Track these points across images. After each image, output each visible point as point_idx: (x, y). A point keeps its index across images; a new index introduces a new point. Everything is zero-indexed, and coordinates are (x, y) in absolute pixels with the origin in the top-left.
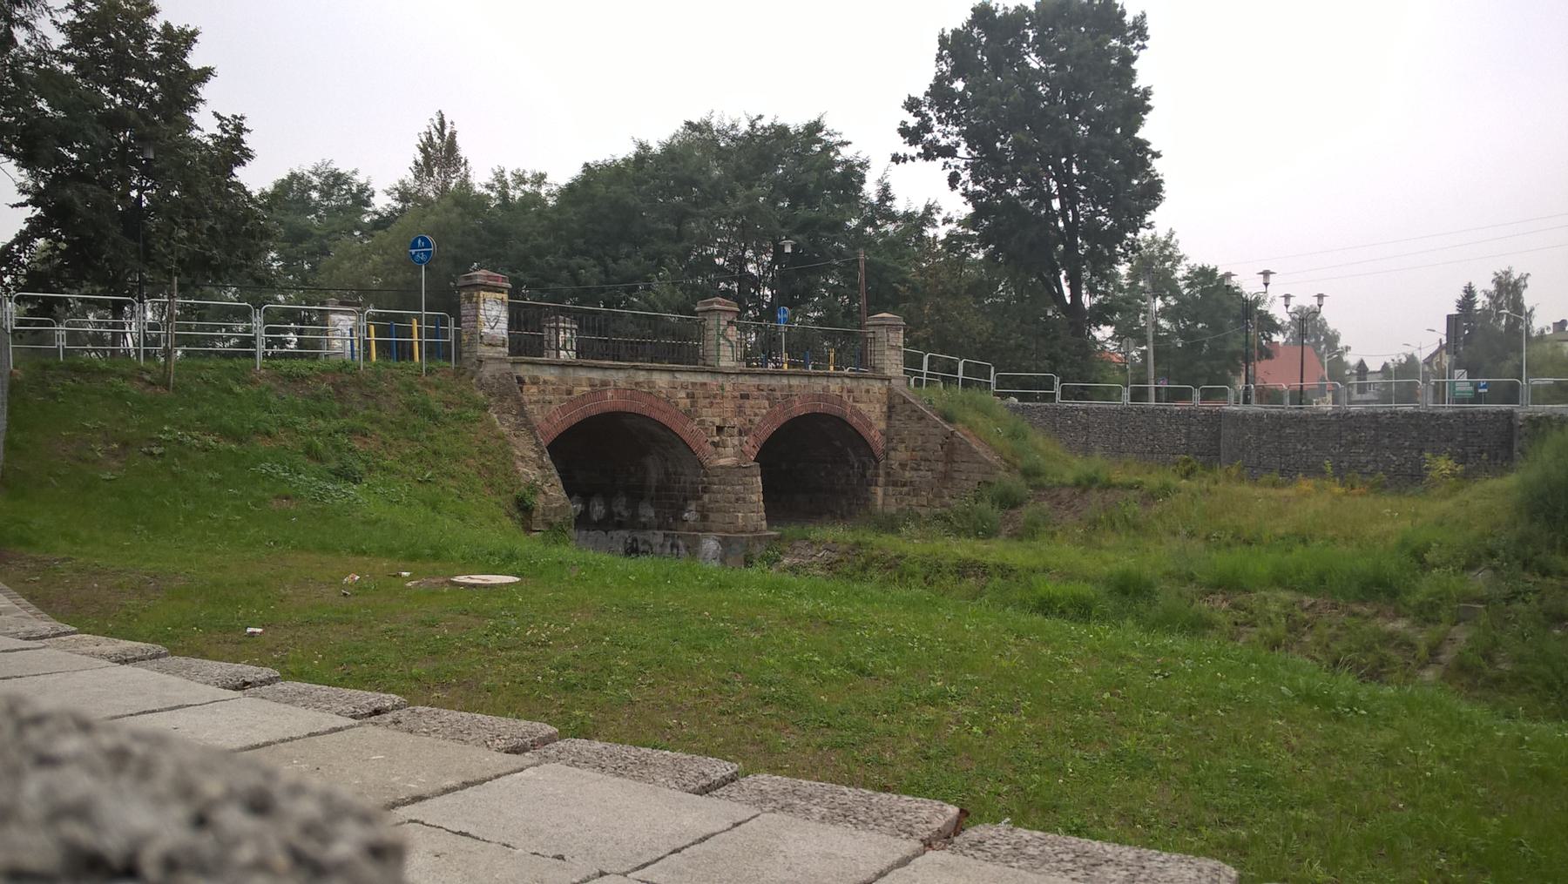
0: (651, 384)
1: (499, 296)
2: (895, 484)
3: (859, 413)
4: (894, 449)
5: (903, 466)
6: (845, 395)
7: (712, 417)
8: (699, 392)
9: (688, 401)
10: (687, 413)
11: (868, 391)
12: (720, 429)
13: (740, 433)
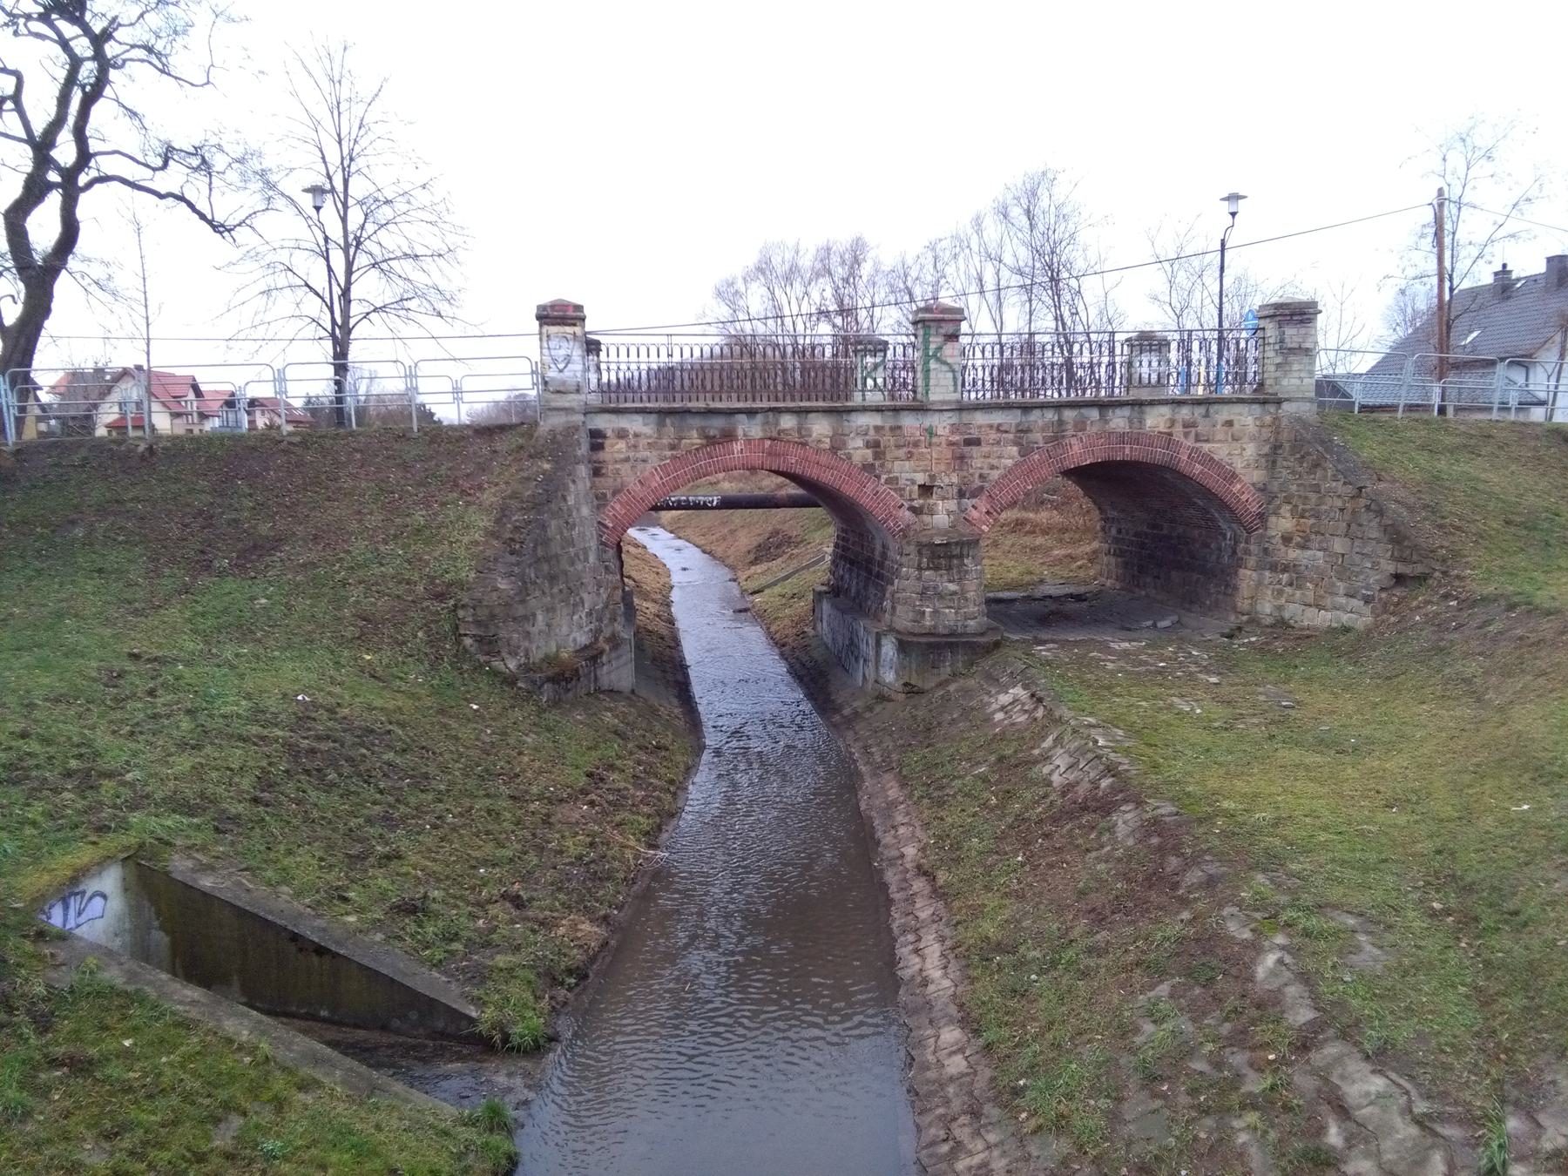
1: (569, 329)
2: (1273, 568)
3: (1208, 460)
4: (1276, 514)
5: (1287, 539)
6: (1178, 431)
7: (910, 473)
8: (887, 440)
9: (869, 452)
10: (867, 468)
11: (1230, 423)
12: (926, 490)
13: (961, 494)
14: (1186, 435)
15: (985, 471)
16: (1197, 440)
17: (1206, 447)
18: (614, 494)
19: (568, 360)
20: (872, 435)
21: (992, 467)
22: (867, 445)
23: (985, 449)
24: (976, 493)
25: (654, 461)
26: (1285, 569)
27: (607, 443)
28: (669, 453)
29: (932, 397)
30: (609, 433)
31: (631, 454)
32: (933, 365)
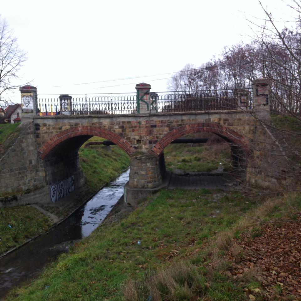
0: (101, 123)
1: (29, 94)
3: (233, 132)
6: (222, 123)
7: (135, 136)
8: (126, 125)
9: (120, 130)
10: (121, 134)
12: (139, 141)
14: (225, 123)
15: (158, 135)
16: (228, 125)
17: (231, 127)
18: (43, 143)
19: (29, 102)
20: (121, 124)
21: (160, 134)
22: (120, 127)
23: (158, 128)
24: (155, 142)
25: (54, 133)
26: (258, 168)
27: (41, 128)
28: (59, 131)
29: (141, 112)
30: (41, 125)
31: (48, 131)
32: (140, 102)
